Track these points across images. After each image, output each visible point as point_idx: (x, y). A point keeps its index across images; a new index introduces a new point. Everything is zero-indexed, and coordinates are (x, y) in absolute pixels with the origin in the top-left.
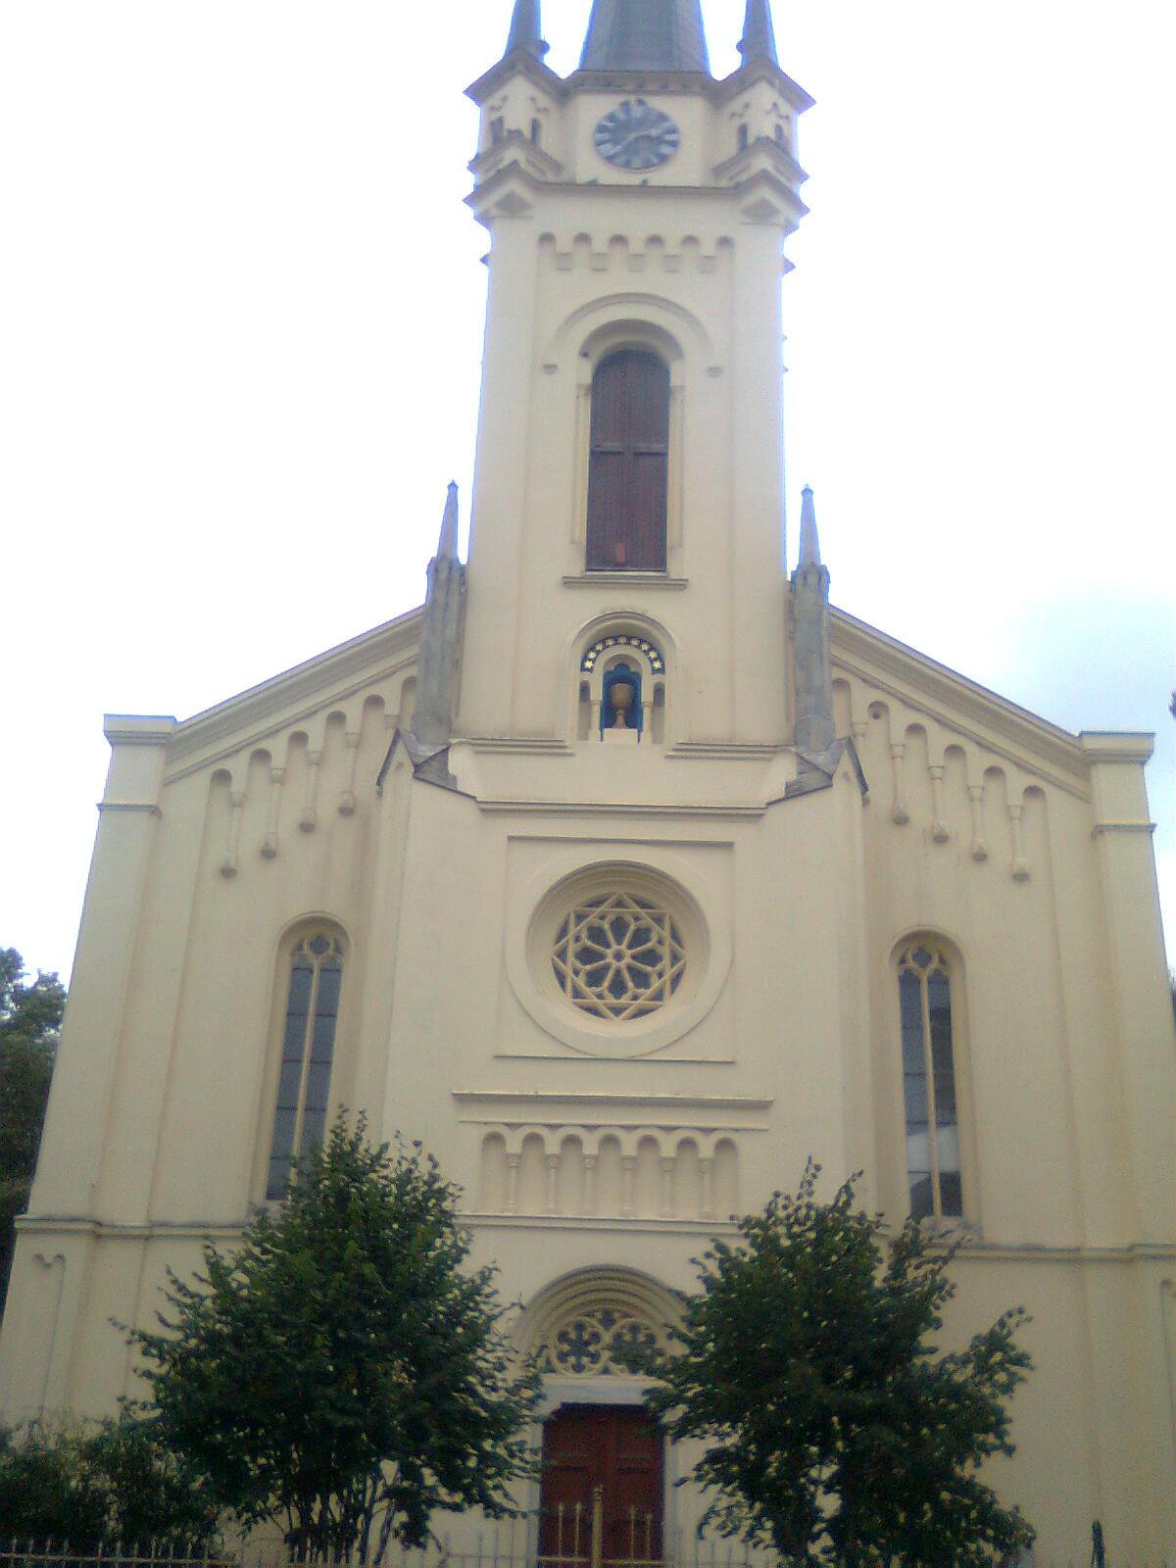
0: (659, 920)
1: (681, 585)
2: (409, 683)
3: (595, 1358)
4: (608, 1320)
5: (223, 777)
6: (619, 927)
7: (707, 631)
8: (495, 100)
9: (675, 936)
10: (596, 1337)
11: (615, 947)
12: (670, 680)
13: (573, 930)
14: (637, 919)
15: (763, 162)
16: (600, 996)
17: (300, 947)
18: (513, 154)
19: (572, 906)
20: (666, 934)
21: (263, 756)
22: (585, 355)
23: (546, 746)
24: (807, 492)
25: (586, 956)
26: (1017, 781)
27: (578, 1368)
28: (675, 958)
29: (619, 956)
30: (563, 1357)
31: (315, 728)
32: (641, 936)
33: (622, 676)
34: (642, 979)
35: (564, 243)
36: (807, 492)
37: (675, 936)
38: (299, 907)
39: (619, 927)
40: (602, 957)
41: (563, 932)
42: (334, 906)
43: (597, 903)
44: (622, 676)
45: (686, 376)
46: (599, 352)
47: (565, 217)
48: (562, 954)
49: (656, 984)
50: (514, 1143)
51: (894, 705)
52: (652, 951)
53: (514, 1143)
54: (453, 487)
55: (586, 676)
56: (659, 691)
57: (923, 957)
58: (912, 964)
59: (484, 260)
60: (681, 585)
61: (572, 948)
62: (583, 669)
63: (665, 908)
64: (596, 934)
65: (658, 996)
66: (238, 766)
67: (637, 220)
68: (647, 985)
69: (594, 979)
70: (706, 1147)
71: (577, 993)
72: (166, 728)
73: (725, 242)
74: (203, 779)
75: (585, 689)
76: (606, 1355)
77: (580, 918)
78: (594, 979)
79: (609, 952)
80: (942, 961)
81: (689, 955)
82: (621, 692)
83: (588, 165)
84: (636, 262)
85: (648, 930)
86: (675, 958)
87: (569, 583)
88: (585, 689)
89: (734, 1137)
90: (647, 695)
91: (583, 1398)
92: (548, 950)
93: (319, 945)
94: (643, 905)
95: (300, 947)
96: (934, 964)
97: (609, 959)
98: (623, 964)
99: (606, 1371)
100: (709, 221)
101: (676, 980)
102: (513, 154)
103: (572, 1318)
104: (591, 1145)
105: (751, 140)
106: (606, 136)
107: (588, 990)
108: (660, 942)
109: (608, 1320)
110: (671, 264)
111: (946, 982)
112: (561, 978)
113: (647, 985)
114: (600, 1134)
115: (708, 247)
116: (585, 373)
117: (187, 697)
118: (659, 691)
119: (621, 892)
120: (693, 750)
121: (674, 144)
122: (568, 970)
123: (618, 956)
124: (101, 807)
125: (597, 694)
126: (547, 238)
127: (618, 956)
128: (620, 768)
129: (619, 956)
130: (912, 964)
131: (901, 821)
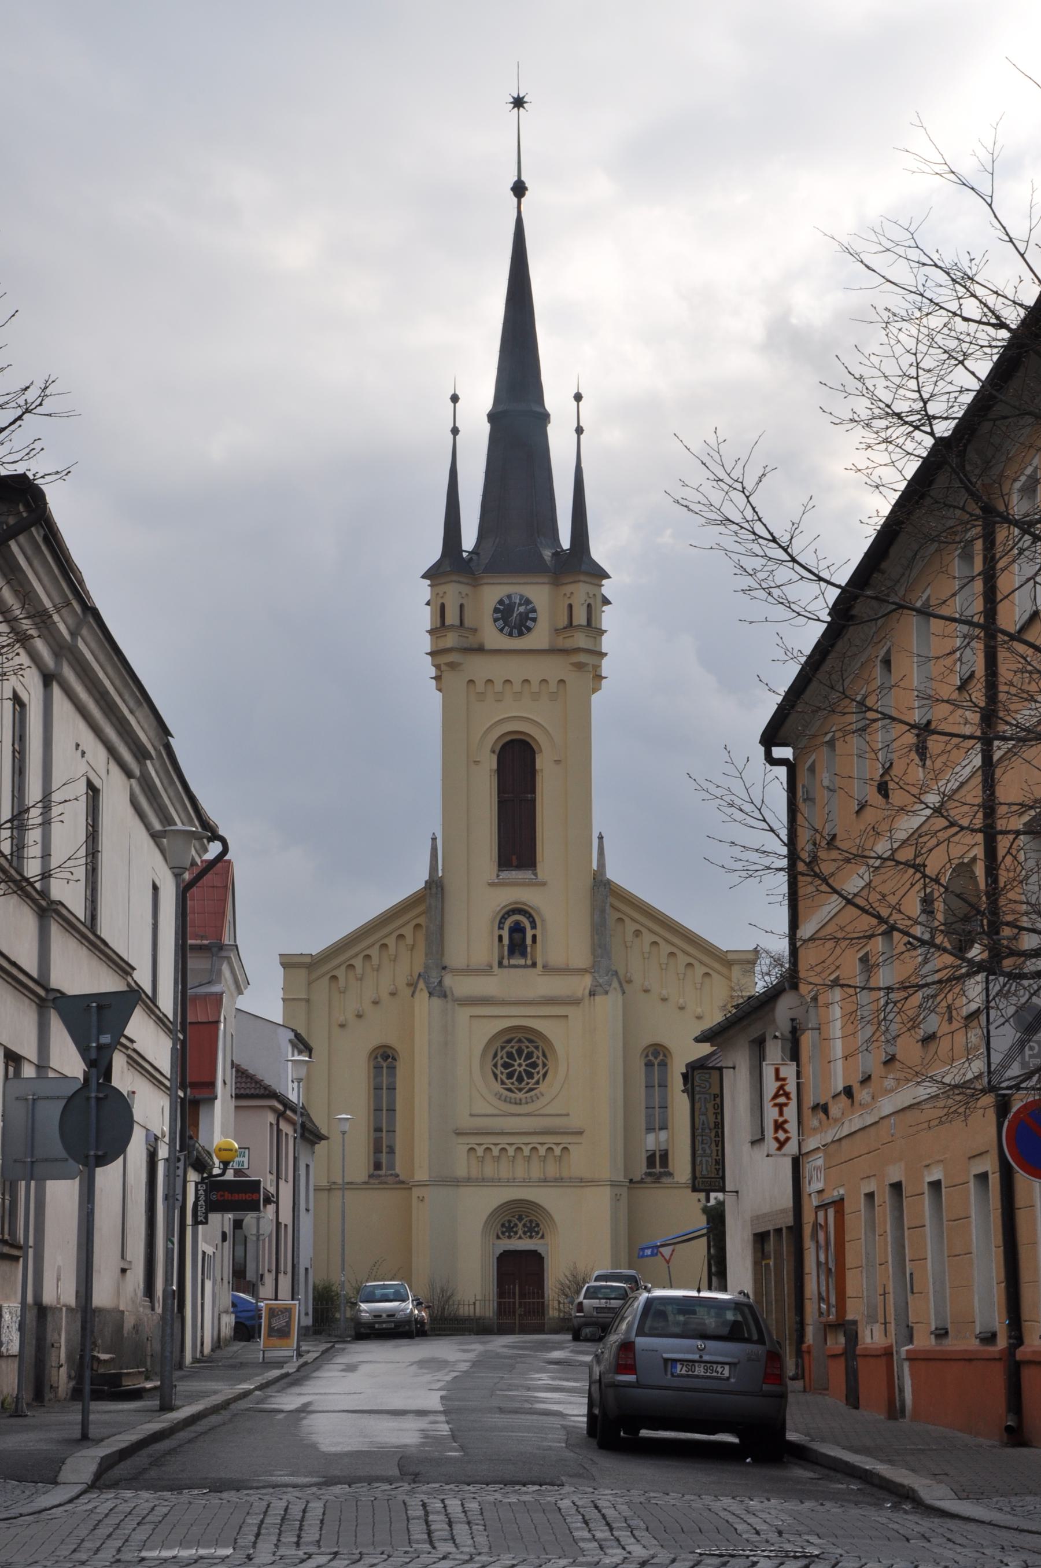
0: (537, 1048)
2: (418, 926)
3: (516, 1233)
4: (520, 1219)
5: (334, 978)
6: (520, 1052)
8: (441, 589)
9: (544, 1055)
10: (516, 1225)
11: (518, 1061)
12: (538, 932)
14: (527, 1047)
15: (581, 640)
16: (512, 1084)
17: (376, 1058)
18: (451, 640)
19: (498, 1044)
20: (540, 1055)
21: (351, 966)
22: (493, 752)
23: (486, 971)
24: (601, 838)
25: (506, 1065)
26: (700, 970)
27: (510, 1237)
28: (544, 1065)
29: (520, 1065)
31: (374, 952)
32: (530, 1055)
33: (517, 930)
34: (530, 1076)
35: (480, 687)
36: (601, 838)
37: (544, 1055)
38: (376, 1039)
39: (520, 1052)
40: (513, 1065)
41: (495, 1055)
42: (392, 1040)
43: (509, 1041)
44: (517, 930)
45: (543, 762)
46: (498, 749)
47: (479, 668)
48: (495, 1066)
50: (480, 1151)
52: (534, 1062)
53: (480, 1151)
54: (434, 839)
55: (501, 932)
56: (534, 937)
57: (656, 1054)
58: (651, 1058)
59: (428, 604)
61: (500, 1062)
62: (500, 928)
63: (540, 1044)
64: (510, 1055)
65: (537, 1083)
66: (340, 973)
67: (515, 669)
68: (532, 1078)
69: (510, 1076)
70: (557, 1151)
71: (503, 1083)
72: (308, 960)
73: (562, 681)
74: (326, 980)
75: (500, 938)
76: (520, 1232)
77: (503, 1048)
78: (510, 1076)
79: (516, 1064)
80: (665, 1055)
81: (550, 1064)
82: (516, 936)
83: (493, 637)
85: (532, 1052)
86: (544, 1065)
87: (492, 885)
88: (500, 938)
89: (569, 1146)
90: (529, 941)
91: (512, 1248)
92: (489, 1064)
93: (386, 1057)
94: (530, 1041)
95: (376, 1058)
96: (661, 1057)
97: (516, 1067)
98: (522, 1069)
99: (520, 1238)
100: (554, 668)
101: (545, 1075)
102: (451, 640)
103: (507, 1218)
104: (511, 1151)
105: (575, 623)
106: (499, 615)
107: (507, 1081)
108: (538, 1058)
109: (520, 1219)
110: (536, 696)
111: (665, 1065)
112: (495, 1076)
113: (532, 1078)
114: (514, 1147)
115: (553, 686)
116: (493, 762)
117: (315, 946)
118: (534, 937)
119: (520, 1035)
120: (549, 970)
121: (534, 620)
123: (520, 1065)
124: (284, 1000)
125: (506, 941)
126: (471, 681)
127: (520, 1065)
130: (651, 1058)
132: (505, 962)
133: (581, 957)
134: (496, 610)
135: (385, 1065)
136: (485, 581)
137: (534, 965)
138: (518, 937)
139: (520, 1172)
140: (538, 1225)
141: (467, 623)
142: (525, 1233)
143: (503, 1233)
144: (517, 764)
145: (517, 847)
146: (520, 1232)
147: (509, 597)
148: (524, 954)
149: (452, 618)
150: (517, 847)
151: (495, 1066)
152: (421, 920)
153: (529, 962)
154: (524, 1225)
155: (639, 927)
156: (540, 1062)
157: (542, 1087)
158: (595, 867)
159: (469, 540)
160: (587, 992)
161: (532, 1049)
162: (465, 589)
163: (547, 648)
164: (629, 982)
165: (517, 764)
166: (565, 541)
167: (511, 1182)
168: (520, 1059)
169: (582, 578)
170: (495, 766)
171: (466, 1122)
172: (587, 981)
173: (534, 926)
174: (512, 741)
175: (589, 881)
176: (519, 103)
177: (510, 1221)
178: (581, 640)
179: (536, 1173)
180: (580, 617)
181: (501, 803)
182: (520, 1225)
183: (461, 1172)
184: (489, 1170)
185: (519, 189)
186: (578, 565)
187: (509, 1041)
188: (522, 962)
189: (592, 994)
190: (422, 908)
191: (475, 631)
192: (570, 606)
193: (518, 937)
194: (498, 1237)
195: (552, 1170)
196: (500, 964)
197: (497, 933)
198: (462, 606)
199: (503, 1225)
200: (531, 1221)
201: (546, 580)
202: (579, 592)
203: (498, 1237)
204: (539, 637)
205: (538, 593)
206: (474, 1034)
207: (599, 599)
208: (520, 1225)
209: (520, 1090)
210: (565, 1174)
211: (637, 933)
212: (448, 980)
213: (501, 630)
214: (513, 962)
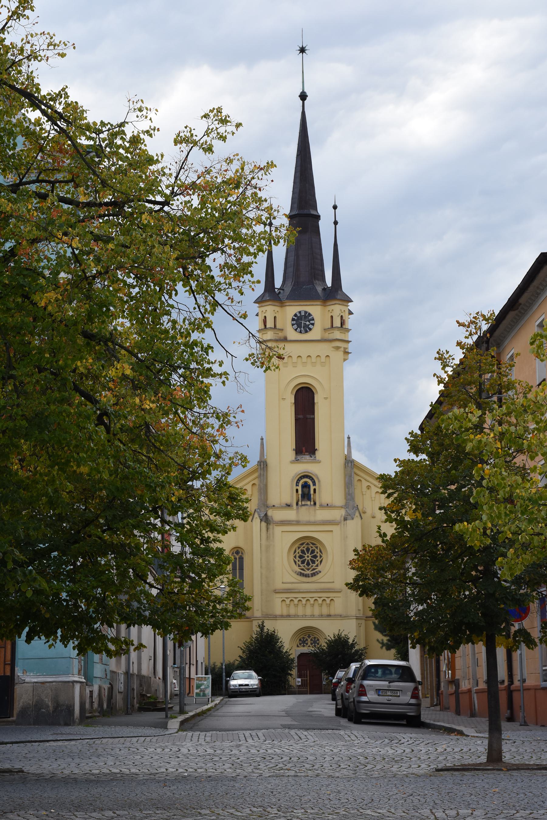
0: (317, 547)
1: (319, 462)
3: (307, 644)
4: (309, 637)
6: (308, 550)
7: (325, 468)
9: (321, 551)
10: (307, 640)
12: (317, 487)
13: (297, 551)
15: (337, 335)
18: (269, 335)
19: (297, 546)
24: (349, 438)
27: (304, 646)
28: (321, 557)
29: (308, 557)
30: (300, 644)
32: (313, 551)
33: (306, 486)
34: (313, 562)
36: (349, 438)
39: (308, 550)
42: (241, 545)
43: (302, 544)
44: (306, 486)
45: (318, 399)
48: (295, 557)
49: (316, 563)
50: (288, 601)
51: (372, 486)
56: (315, 490)
60: (319, 462)
61: (298, 555)
63: (318, 545)
64: (303, 552)
65: (317, 566)
70: (328, 601)
71: (299, 566)
75: (297, 491)
76: (309, 644)
77: (299, 548)
78: (303, 562)
82: (306, 490)
83: (292, 334)
84: (304, 364)
86: (321, 557)
88: (297, 491)
90: (312, 492)
93: (237, 553)
94: (313, 544)
100: (324, 349)
104: (304, 601)
105: (334, 326)
106: (295, 322)
109: (309, 637)
110: (314, 364)
112: (295, 562)
115: (323, 359)
118: (315, 490)
119: (308, 541)
122: (297, 561)
123: (308, 557)
125: (300, 492)
127: (308, 557)
128: (306, 513)
129: (308, 557)
131: (374, 517)
132: (300, 503)
133: (339, 499)
134: (293, 320)
135: (237, 557)
136: (287, 304)
137: (315, 504)
138: (306, 490)
139: (309, 611)
140: (318, 640)
141: (278, 326)
142: (311, 644)
143: (300, 644)
144: (304, 400)
145: (305, 442)
146: (309, 644)
147: (300, 312)
148: (309, 499)
149: (270, 324)
150: (305, 442)
151: (295, 557)
152: (255, 481)
153: (312, 503)
154: (311, 640)
155: (369, 484)
156: (318, 555)
157: (319, 568)
158: (346, 453)
159: (278, 282)
160: (343, 518)
161: (314, 548)
162: (277, 309)
163: (319, 338)
164: (364, 513)
165: (304, 400)
166: (329, 282)
167: (304, 616)
168: (308, 554)
169: (337, 302)
170: (293, 401)
171: (279, 586)
172: (343, 512)
173: (314, 484)
174: (302, 388)
175: (342, 461)
176: (302, 50)
177: (303, 638)
178: (337, 335)
179: (317, 612)
180: (337, 323)
181: (296, 420)
182: (309, 640)
183: (278, 612)
184: (292, 611)
185: (303, 97)
186: (335, 293)
187: (302, 544)
188: (309, 503)
189: (345, 519)
190: (256, 475)
191: (282, 330)
192: (332, 317)
193: (306, 490)
194: (298, 646)
195: (325, 611)
196: (297, 504)
197: (295, 488)
198: (275, 317)
199: (300, 640)
200: (315, 638)
201: (319, 303)
202: (336, 309)
203: (298, 646)
204: (316, 333)
205: (315, 310)
206: (284, 540)
207: (347, 312)
208: (309, 640)
209: (308, 569)
210: (332, 613)
211: (368, 487)
212: (270, 513)
213: (296, 330)
214: (303, 503)
